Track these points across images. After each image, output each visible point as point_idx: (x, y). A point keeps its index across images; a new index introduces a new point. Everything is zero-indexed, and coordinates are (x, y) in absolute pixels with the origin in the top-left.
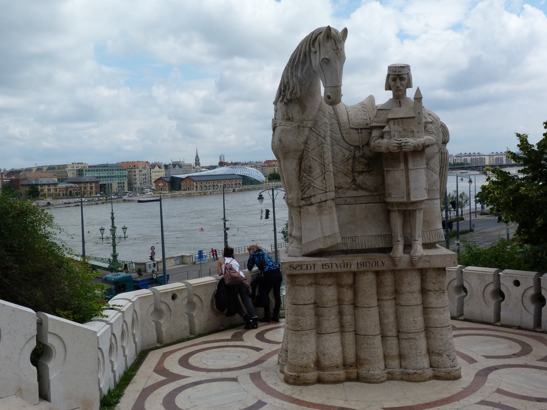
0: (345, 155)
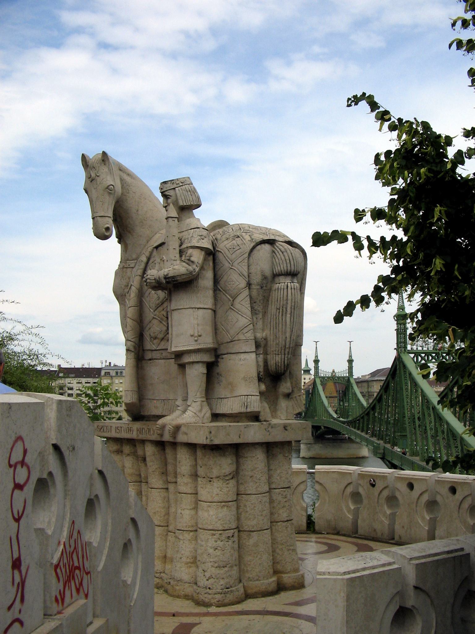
0: (160, 298)
